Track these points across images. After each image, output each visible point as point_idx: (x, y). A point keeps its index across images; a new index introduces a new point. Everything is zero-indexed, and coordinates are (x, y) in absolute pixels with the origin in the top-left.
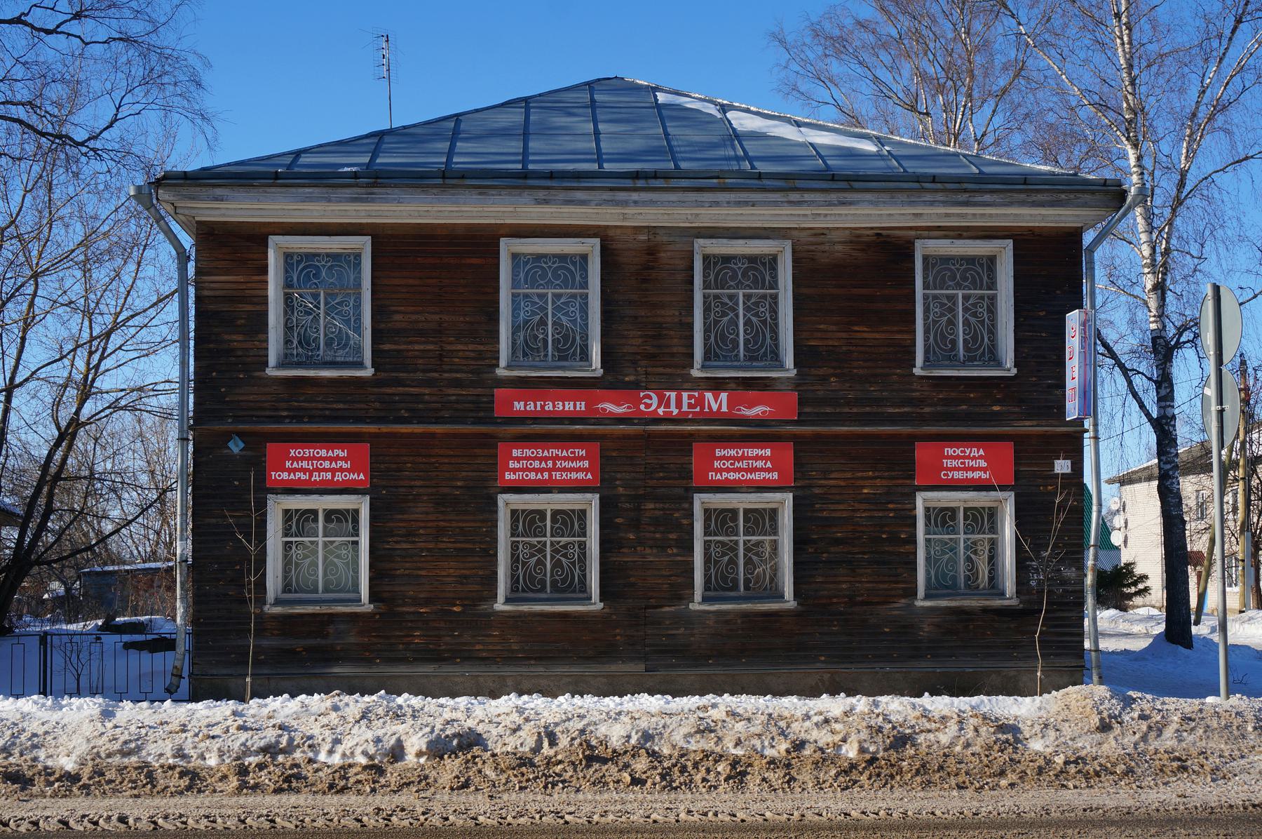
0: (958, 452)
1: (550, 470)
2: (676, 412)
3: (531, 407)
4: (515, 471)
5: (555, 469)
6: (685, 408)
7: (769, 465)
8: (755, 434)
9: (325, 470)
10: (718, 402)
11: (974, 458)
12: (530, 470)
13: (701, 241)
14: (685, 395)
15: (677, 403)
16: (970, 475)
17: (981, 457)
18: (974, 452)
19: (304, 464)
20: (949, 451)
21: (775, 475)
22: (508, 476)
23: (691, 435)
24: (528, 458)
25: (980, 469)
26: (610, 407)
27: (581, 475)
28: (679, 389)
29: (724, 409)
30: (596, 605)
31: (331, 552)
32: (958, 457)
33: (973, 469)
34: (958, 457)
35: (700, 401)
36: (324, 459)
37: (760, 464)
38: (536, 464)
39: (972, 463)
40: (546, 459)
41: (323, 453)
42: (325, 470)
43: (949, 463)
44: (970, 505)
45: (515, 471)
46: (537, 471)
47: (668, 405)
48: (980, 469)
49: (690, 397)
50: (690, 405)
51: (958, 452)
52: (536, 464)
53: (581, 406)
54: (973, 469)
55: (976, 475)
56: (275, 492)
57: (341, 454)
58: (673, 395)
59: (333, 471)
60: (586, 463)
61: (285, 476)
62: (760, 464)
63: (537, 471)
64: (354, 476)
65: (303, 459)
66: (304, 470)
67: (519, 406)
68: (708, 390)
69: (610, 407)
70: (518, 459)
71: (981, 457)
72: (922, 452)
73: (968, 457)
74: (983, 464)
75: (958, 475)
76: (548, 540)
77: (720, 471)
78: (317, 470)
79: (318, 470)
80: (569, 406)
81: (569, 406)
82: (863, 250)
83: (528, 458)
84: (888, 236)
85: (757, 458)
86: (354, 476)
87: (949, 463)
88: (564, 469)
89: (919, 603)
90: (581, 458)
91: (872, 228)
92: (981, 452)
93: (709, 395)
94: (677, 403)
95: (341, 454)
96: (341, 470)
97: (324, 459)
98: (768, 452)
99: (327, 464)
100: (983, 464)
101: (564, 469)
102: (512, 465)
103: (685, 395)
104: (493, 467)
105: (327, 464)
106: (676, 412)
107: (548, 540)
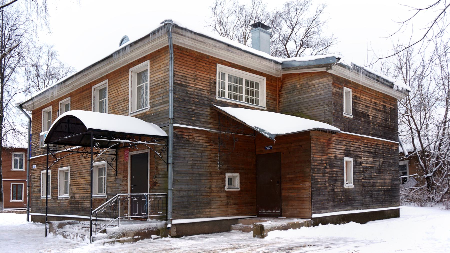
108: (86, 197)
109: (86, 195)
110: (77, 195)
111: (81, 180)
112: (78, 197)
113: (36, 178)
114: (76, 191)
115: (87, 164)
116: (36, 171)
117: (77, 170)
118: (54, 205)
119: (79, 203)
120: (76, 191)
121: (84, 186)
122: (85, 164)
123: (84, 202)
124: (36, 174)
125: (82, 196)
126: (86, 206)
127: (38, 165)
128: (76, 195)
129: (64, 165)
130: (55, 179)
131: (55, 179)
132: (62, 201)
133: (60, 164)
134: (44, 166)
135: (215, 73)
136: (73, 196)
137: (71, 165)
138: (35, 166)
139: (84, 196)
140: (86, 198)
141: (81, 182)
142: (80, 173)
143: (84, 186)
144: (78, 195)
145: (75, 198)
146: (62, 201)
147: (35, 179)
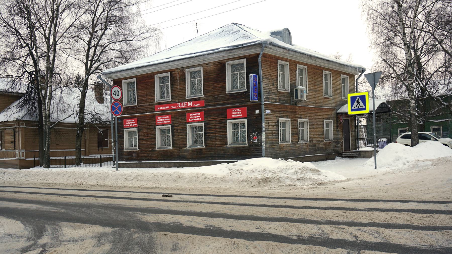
0: (235, 110)
1: (163, 121)
2: (183, 107)
3: (160, 109)
4: (158, 122)
5: (164, 121)
6: (185, 106)
7: (200, 117)
8: (195, 111)
9: (131, 124)
10: (190, 104)
11: (239, 112)
12: (160, 121)
13: (187, 70)
14: (185, 103)
15: (184, 105)
16: (238, 116)
17: (240, 111)
18: (239, 110)
19: (129, 123)
20: (233, 110)
21: (201, 119)
22: (158, 123)
23: (186, 111)
24: (160, 119)
25: (240, 114)
26: (173, 107)
27: (168, 122)
28: (184, 102)
29: (192, 105)
30: (171, 148)
31: (242, 133)
32: (235, 112)
33: (238, 114)
34: (235, 112)
35: (187, 104)
36: (131, 122)
37: (198, 117)
38: (161, 120)
39: (238, 113)
40: (163, 119)
41: (131, 121)
42: (131, 124)
43: (233, 113)
44: (241, 122)
45: (158, 122)
46: (162, 121)
47: (182, 106)
48: (240, 114)
49: (186, 103)
50: (186, 105)
51: (235, 110)
52: (161, 120)
53: (168, 107)
54: (238, 114)
55: (239, 115)
56: (125, 129)
57: (134, 121)
58: (183, 103)
59: (132, 124)
60: (169, 119)
61: (126, 125)
62: (198, 117)
63: (162, 121)
64: (135, 125)
65: (128, 122)
66: (128, 124)
67: (158, 108)
68: (189, 101)
69: (173, 107)
70: (159, 119)
71: (240, 111)
72: (187, 114)
73: (237, 112)
74: (240, 113)
75: (235, 116)
76: (239, 130)
77: (191, 119)
78: (130, 124)
79: (130, 124)
80: (166, 108)
81: (166, 108)
82: (216, 66)
83: (160, 119)
84: (221, 62)
85: (198, 115)
86: (135, 125)
87: (233, 113)
88: (166, 121)
89: (228, 146)
90: (168, 118)
91: (218, 61)
92: (240, 110)
93: (189, 103)
94: (184, 105)
95: (134, 121)
96: (133, 124)
97: (131, 122)
98: (199, 114)
99: (131, 123)
100: (240, 113)
101: (166, 121)
102: (158, 120)
103: (185, 103)
104: (155, 121)
105: (131, 123)
106: (183, 107)
107: (198, 133)
108: (320, 141)
109: (321, 140)
110: (314, 140)
111: (317, 130)
112: (315, 141)
113: (270, 123)
114: (313, 137)
115: (320, 119)
116: (270, 117)
117: (314, 122)
118: (293, 149)
119: (316, 145)
120: (313, 137)
121: (320, 134)
122: (319, 119)
123: (319, 144)
124: (269, 120)
125: (318, 140)
126: (321, 147)
127: (272, 111)
128: (313, 140)
129: (303, 117)
130: (294, 127)
131: (294, 127)
132: (301, 145)
133: (299, 115)
134: (281, 113)
135: (309, 72)
136: (311, 141)
137: (309, 118)
138: (270, 111)
139: (319, 140)
140: (321, 142)
141: (317, 131)
142: (316, 125)
143: (320, 134)
144: (315, 140)
145: (313, 142)
146: (301, 145)
147: (268, 124)
